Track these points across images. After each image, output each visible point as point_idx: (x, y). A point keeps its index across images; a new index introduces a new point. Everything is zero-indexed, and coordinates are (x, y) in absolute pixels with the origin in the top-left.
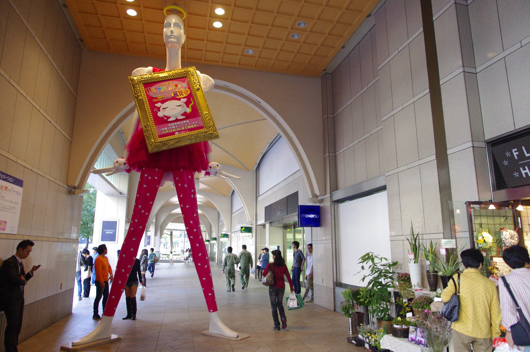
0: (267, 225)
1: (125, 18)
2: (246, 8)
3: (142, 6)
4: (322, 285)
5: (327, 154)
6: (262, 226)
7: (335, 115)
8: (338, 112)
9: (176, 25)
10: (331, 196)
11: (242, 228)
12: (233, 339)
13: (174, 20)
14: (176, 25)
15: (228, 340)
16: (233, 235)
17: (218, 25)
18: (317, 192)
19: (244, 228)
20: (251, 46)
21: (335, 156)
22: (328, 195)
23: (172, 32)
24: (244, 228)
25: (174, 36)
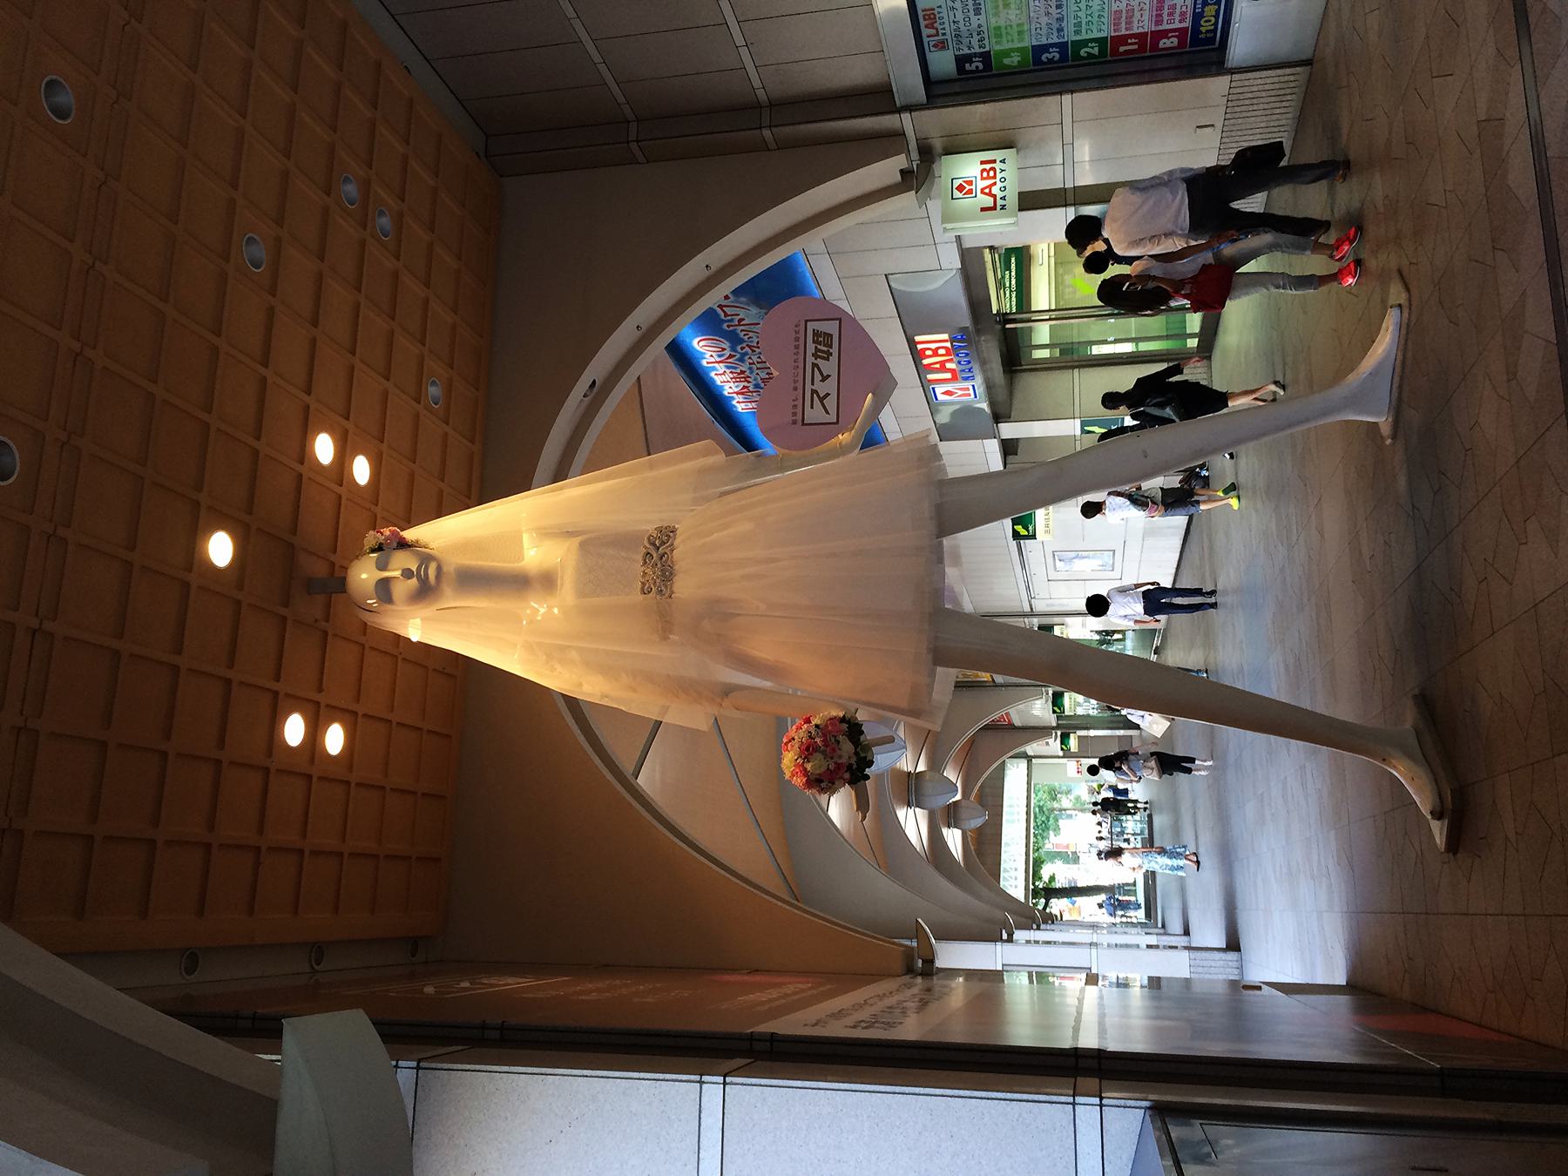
0: (1008, 430)
1: (350, 768)
2: (312, 358)
3: (317, 697)
4: (1219, 125)
5: (767, 133)
6: (1010, 458)
7: (631, 116)
8: (621, 99)
9: (382, 566)
10: (910, 108)
11: (1016, 535)
12: (1406, 315)
13: (364, 576)
14: (382, 566)
15: (1408, 334)
16: (1040, 606)
17: (361, 470)
18: (898, 162)
19: (1019, 528)
20: (420, 383)
21: (771, 105)
22: (906, 116)
23: (407, 574)
24: (1019, 528)
25: (419, 569)
